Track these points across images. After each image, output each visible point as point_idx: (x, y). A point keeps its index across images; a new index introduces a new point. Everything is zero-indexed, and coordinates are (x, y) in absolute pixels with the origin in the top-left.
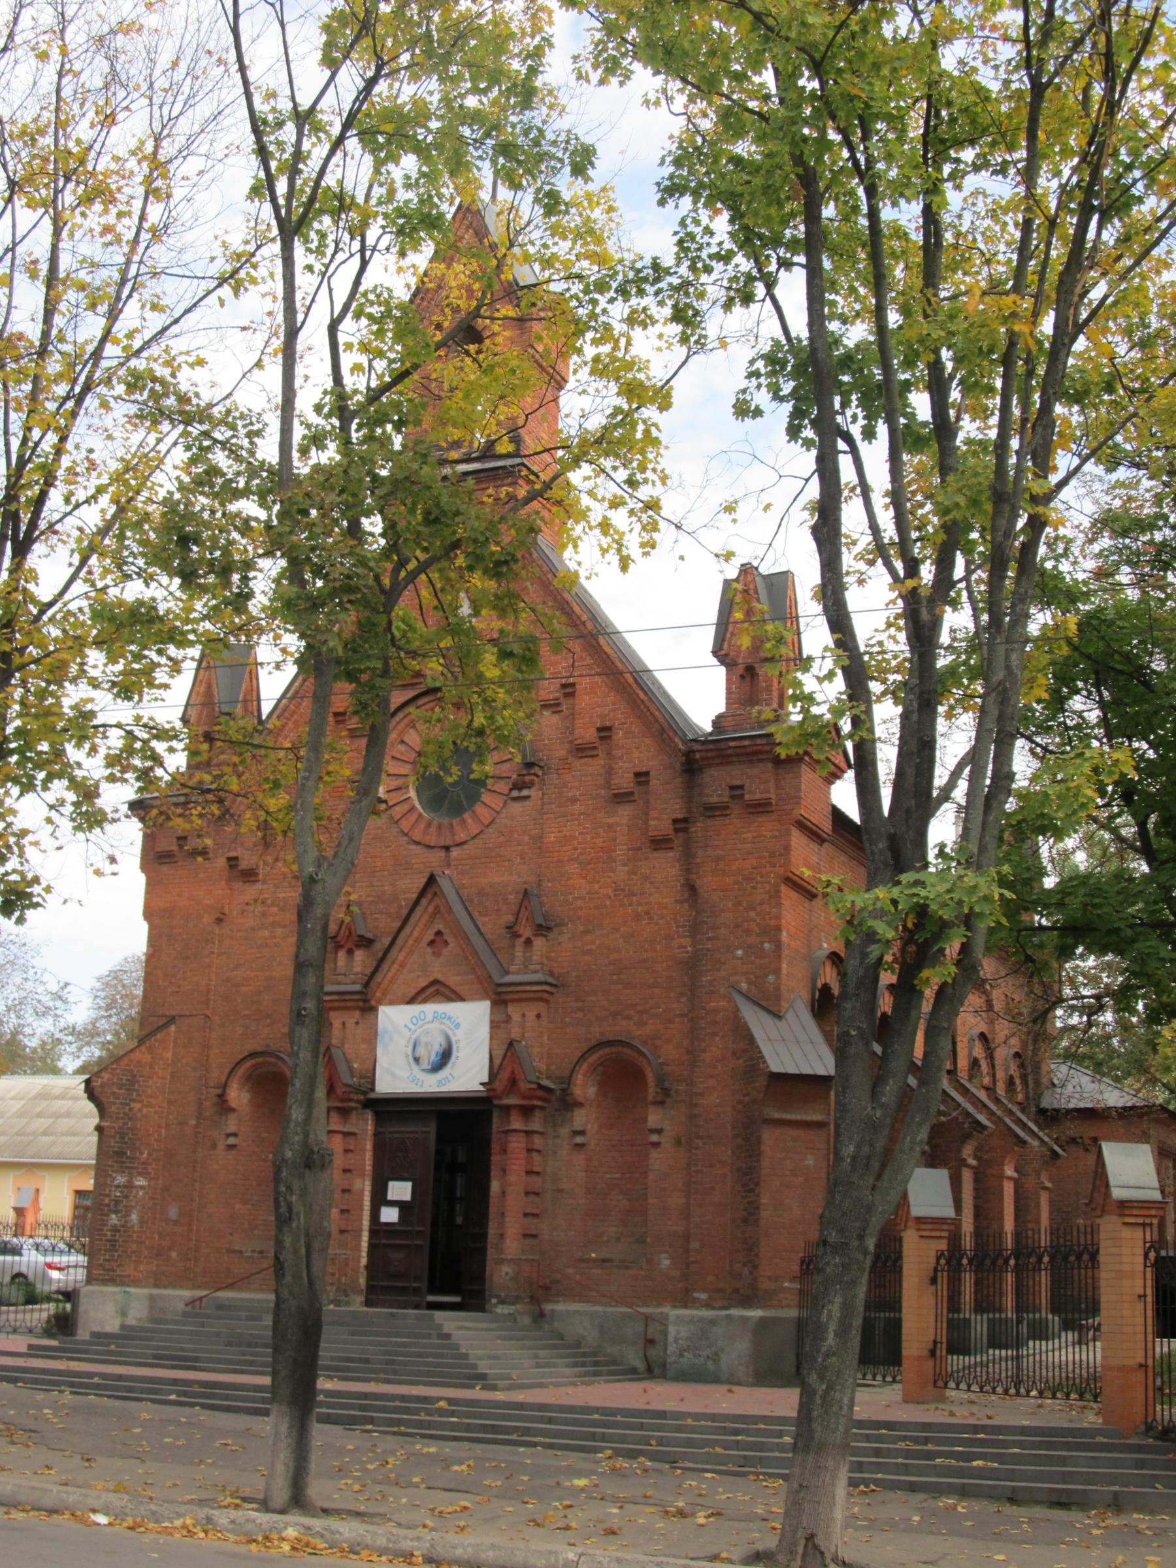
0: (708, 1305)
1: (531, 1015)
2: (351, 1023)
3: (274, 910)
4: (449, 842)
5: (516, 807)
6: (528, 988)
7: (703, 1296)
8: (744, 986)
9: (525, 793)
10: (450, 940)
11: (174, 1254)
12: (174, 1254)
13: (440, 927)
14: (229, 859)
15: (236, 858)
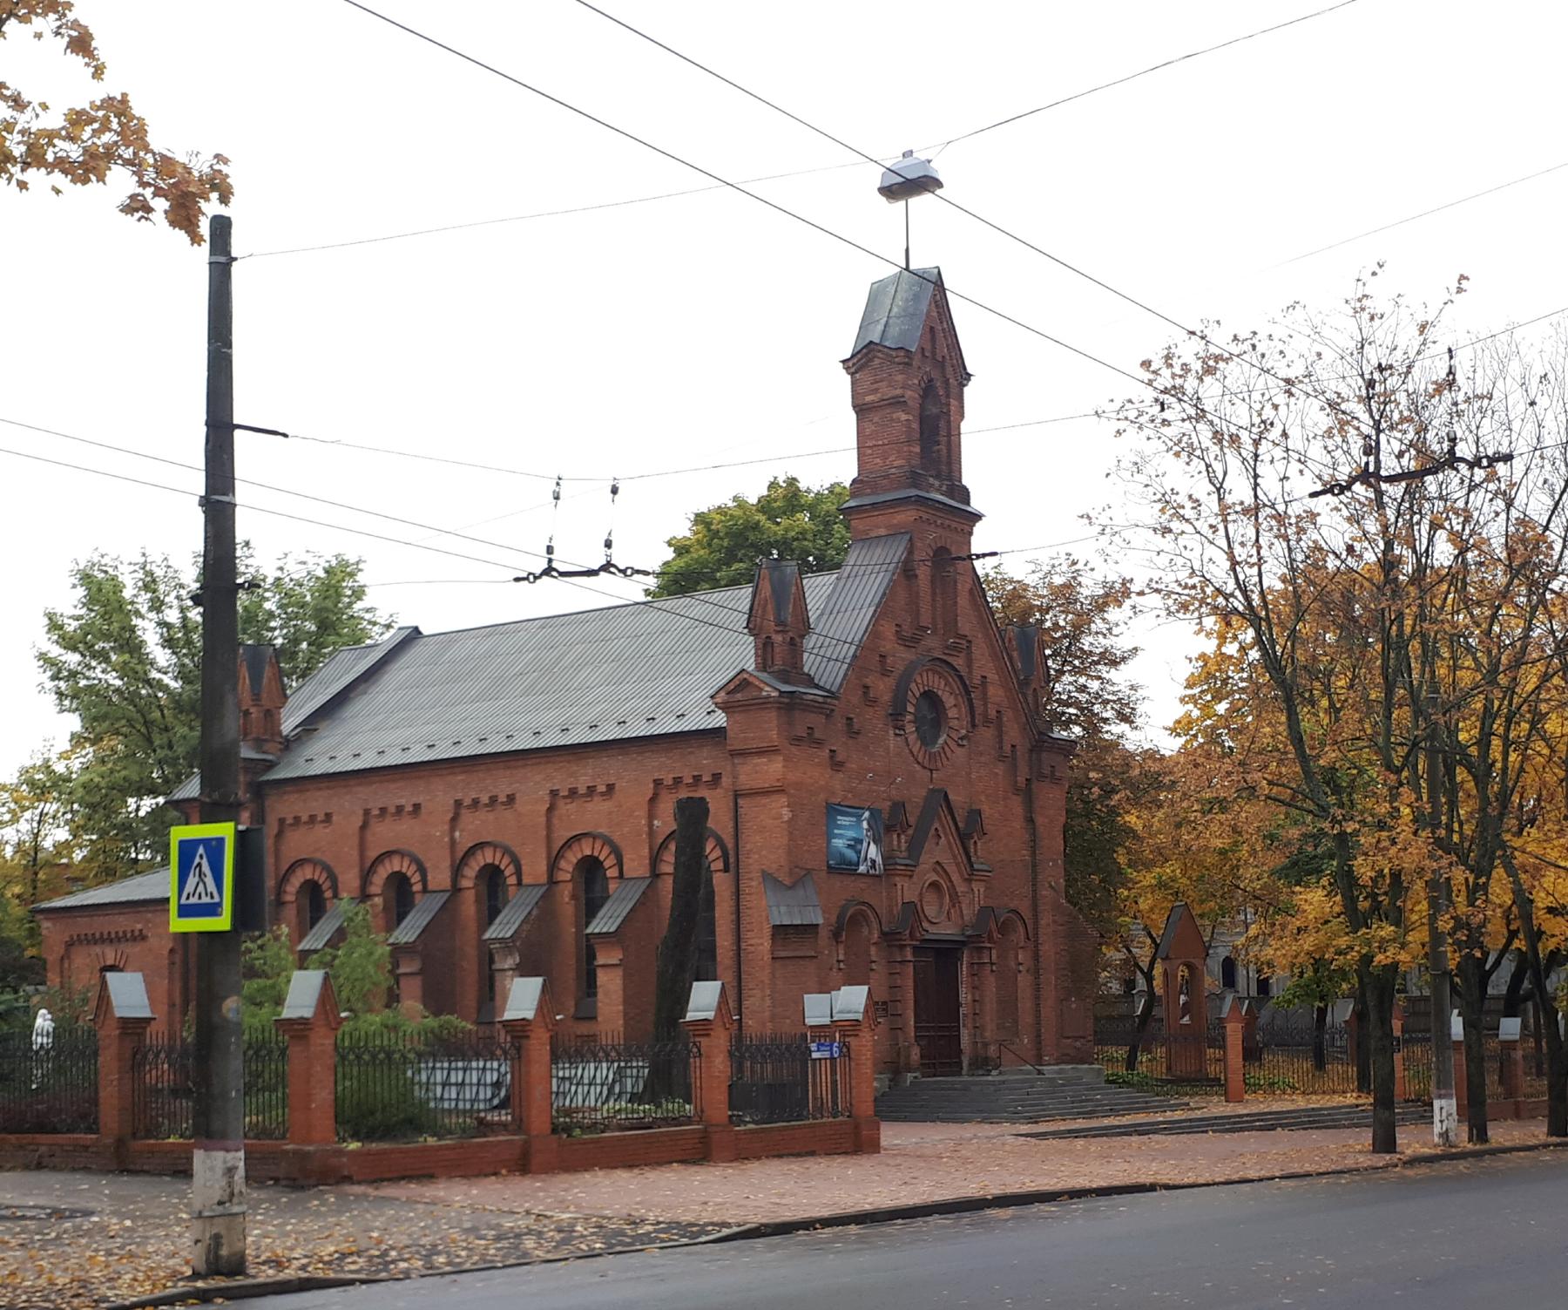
5: (959, 751)
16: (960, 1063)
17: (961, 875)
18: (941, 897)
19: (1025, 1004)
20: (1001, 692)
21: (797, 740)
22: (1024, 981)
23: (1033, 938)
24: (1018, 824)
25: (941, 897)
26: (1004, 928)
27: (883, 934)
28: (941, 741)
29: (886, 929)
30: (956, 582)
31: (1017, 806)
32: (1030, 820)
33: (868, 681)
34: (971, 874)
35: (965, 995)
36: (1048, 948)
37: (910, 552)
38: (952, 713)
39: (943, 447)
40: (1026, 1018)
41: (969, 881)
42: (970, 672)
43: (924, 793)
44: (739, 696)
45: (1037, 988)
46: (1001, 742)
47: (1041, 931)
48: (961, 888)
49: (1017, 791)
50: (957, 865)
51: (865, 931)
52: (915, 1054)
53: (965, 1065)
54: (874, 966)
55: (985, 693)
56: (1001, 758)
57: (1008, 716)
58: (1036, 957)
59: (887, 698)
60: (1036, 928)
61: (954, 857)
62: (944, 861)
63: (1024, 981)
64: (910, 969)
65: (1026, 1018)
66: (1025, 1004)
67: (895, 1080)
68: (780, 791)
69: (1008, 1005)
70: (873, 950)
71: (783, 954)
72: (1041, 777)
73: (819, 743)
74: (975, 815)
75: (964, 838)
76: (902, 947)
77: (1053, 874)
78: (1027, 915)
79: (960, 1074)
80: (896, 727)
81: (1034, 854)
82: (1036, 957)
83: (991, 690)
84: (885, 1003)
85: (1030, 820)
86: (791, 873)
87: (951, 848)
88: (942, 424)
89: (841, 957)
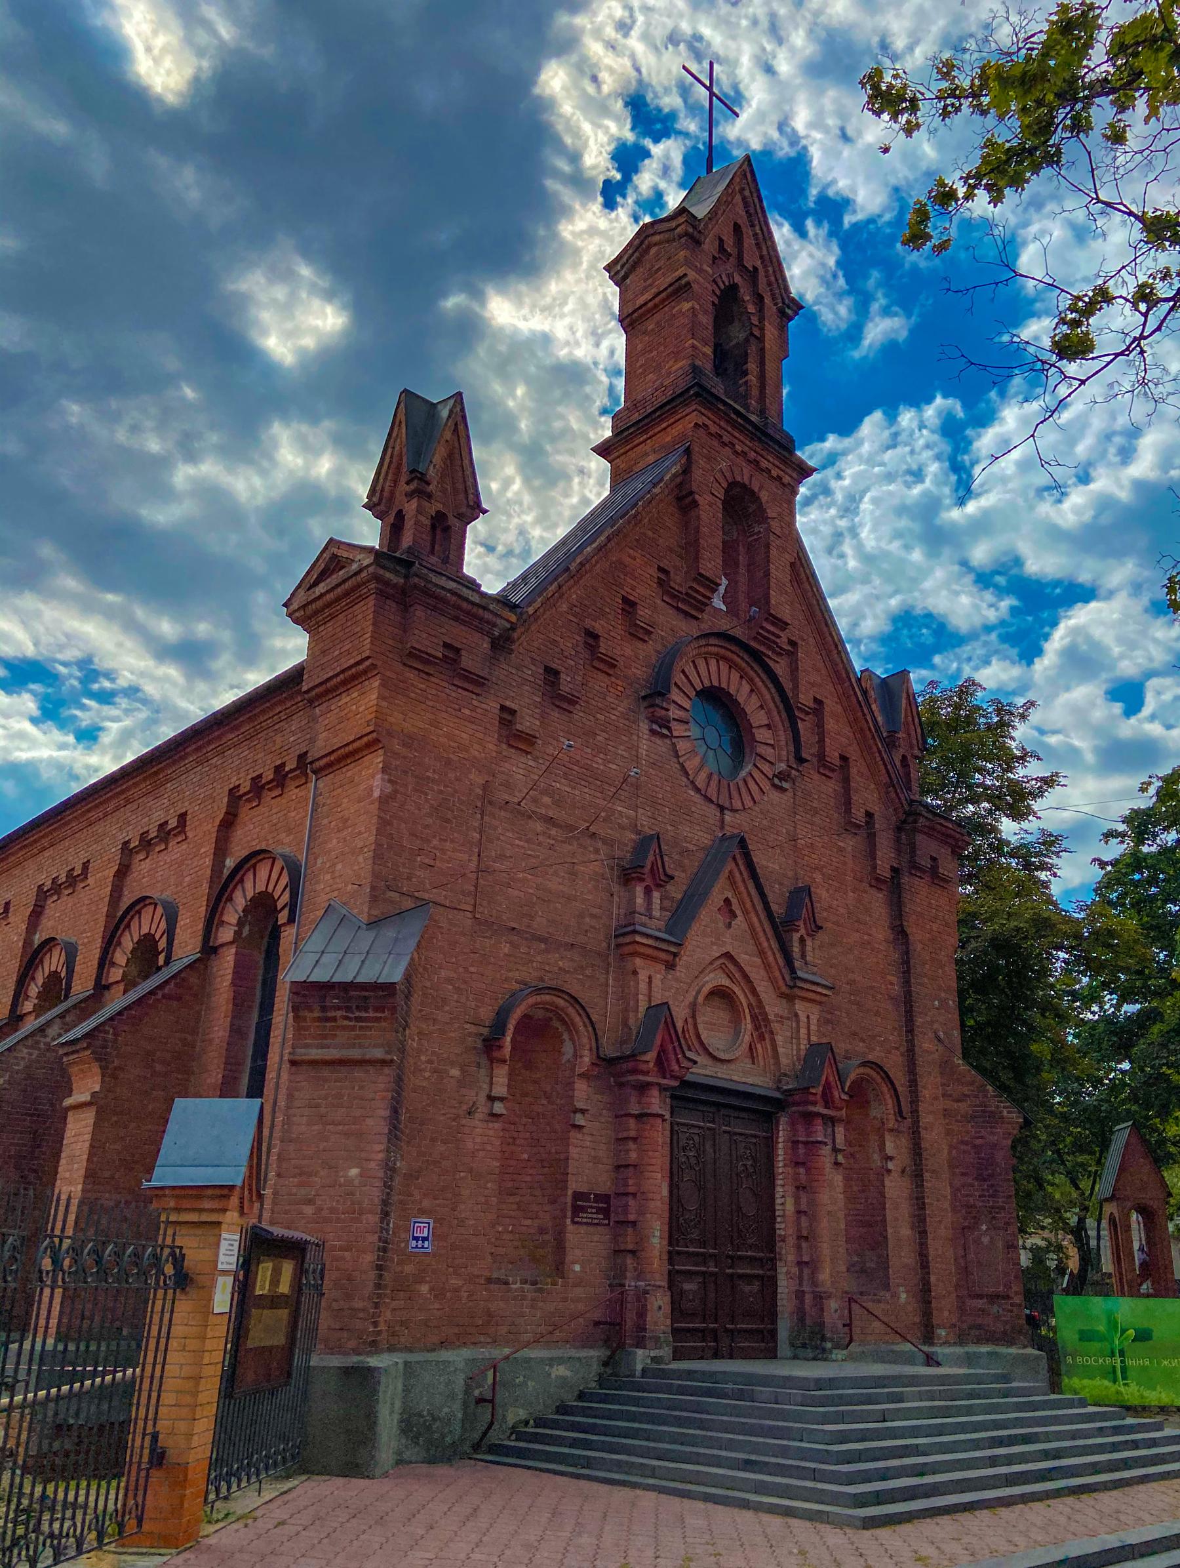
0: (946, 1343)
1: (814, 1019)
2: (657, 978)
3: (547, 800)
4: (727, 805)
5: (775, 795)
6: (820, 990)
7: (943, 1332)
8: (941, 1034)
9: (785, 785)
10: (738, 912)
11: (424, 1289)
12: (424, 1289)
13: (729, 895)
14: (503, 708)
15: (513, 712)
16: (773, 1334)
17: (776, 988)
18: (736, 1019)
19: (900, 1229)
20: (847, 731)
21: (417, 659)
22: (896, 1188)
23: (909, 1115)
24: (881, 933)
25: (736, 1019)
26: (859, 1094)
27: (606, 1063)
28: (743, 773)
29: (609, 1051)
30: (768, 546)
31: (877, 901)
32: (900, 934)
33: (598, 627)
34: (792, 987)
35: (785, 1203)
36: (935, 1136)
37: (686, 470)
38: (762, 735)
39: (752, 378)
40: (901, 1257)
41: (790, 998)
42: (796, 687)
43: (706, 839)
44: (321, 588)
45: (919, 1203)
46: (848, 803)
47: (922, 1107)
48: (774, 1007)
49: (877, 882)
50: (767, 966)
51: (568, 1048)
52: (659, 1305)
53: (783, 1334)
54: (579, 1120)
55: (820, 725)
56: (850, 826)
57: (857, 769)
58: (917, 1151)
59: (639, 672)
60: (915, 1101)
61: (761, 953)
62: (743, 958)
63: (896, 1188)
64: (660, 1134)
65: (901, 1257)
66: (900, 1229)
67: (613, 1369)
68: (372, 745)
69: (868, 1229)
70: (582, 1091)
71: (315, 1054)
72: (914, 866)
73: (476, 682)
74: (801, 896)
75: (781, 929)
76: (643, 1088)
77: (940, 1020)
78: (900, 1079)
79: (771, 1354)
80: (653, 720)
81: (907, 983)
82: (917, 1151)
83: (830, 724)
84: (605, 1198)
85: (900, 934)
86: (374, 899)
87: (754, 936)
88: (753, 349)
89: (500, 1090)
